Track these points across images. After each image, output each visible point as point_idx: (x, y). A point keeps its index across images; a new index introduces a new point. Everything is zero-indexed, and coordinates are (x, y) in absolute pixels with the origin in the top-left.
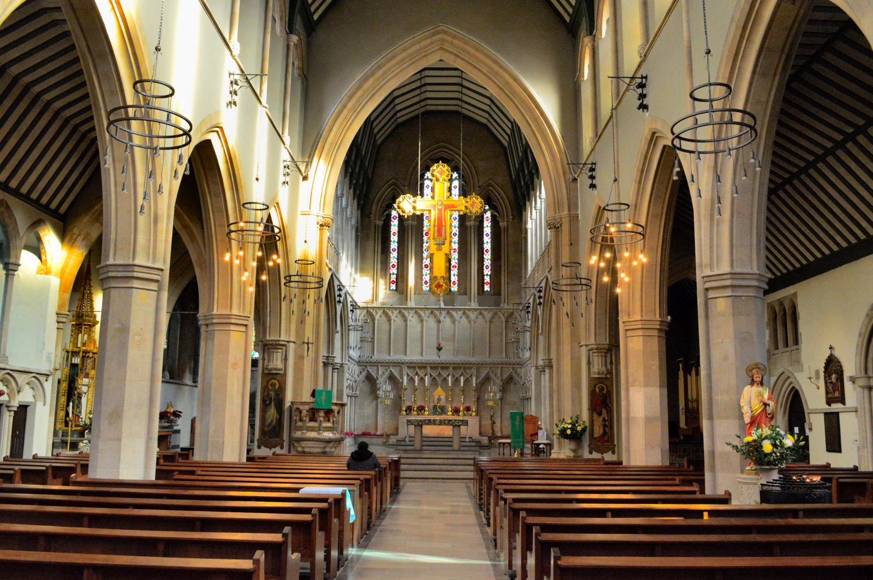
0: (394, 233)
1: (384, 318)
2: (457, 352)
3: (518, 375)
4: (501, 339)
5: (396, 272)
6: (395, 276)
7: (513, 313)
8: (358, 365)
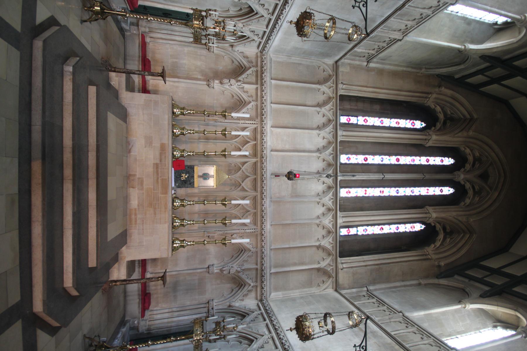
0: (399, 123)
1: (321, 98)
2: (278, 202)
3: (246, 295)
4: (295, 264)
5: (359, 123)
6: (355, 122)
7: (330, 276)
8: (257, 53)
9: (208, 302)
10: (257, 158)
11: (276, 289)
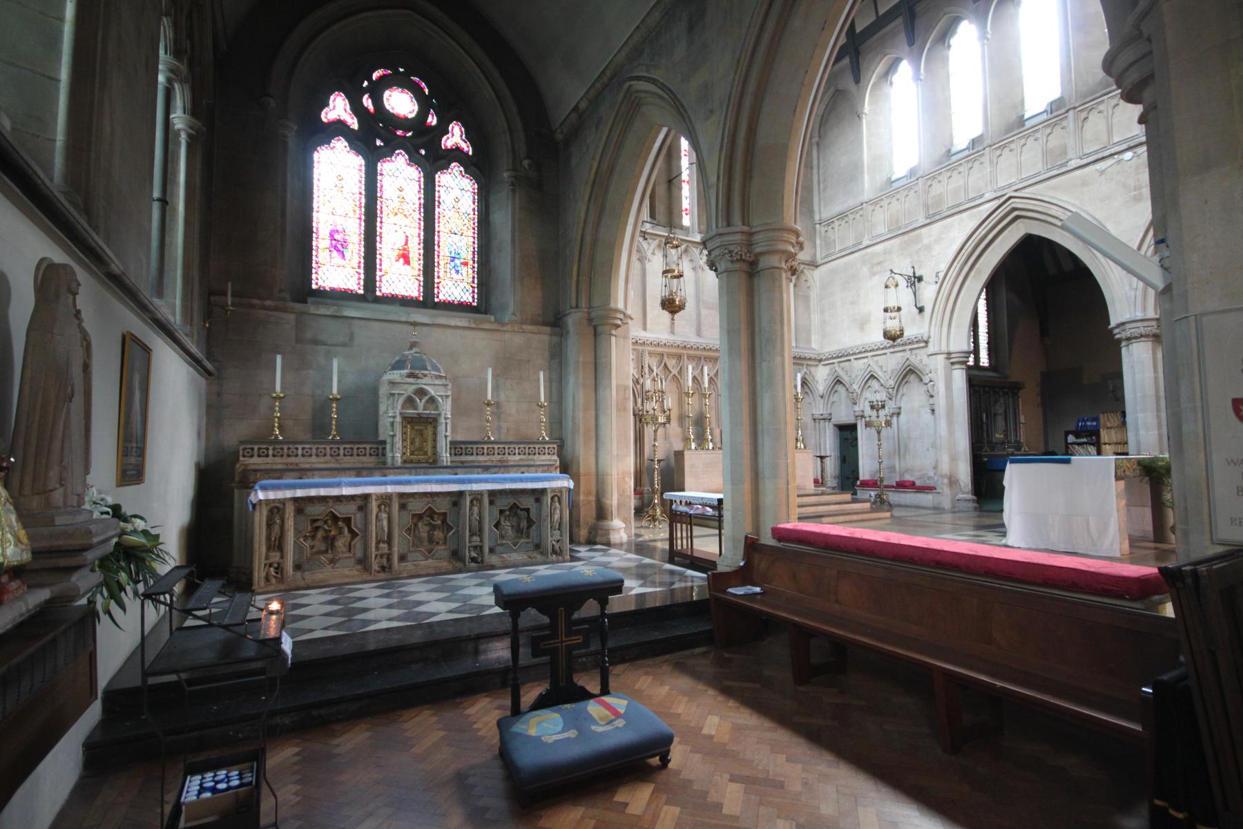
9: (814, 420)
10: (683, 354)
11: (809, 341)
